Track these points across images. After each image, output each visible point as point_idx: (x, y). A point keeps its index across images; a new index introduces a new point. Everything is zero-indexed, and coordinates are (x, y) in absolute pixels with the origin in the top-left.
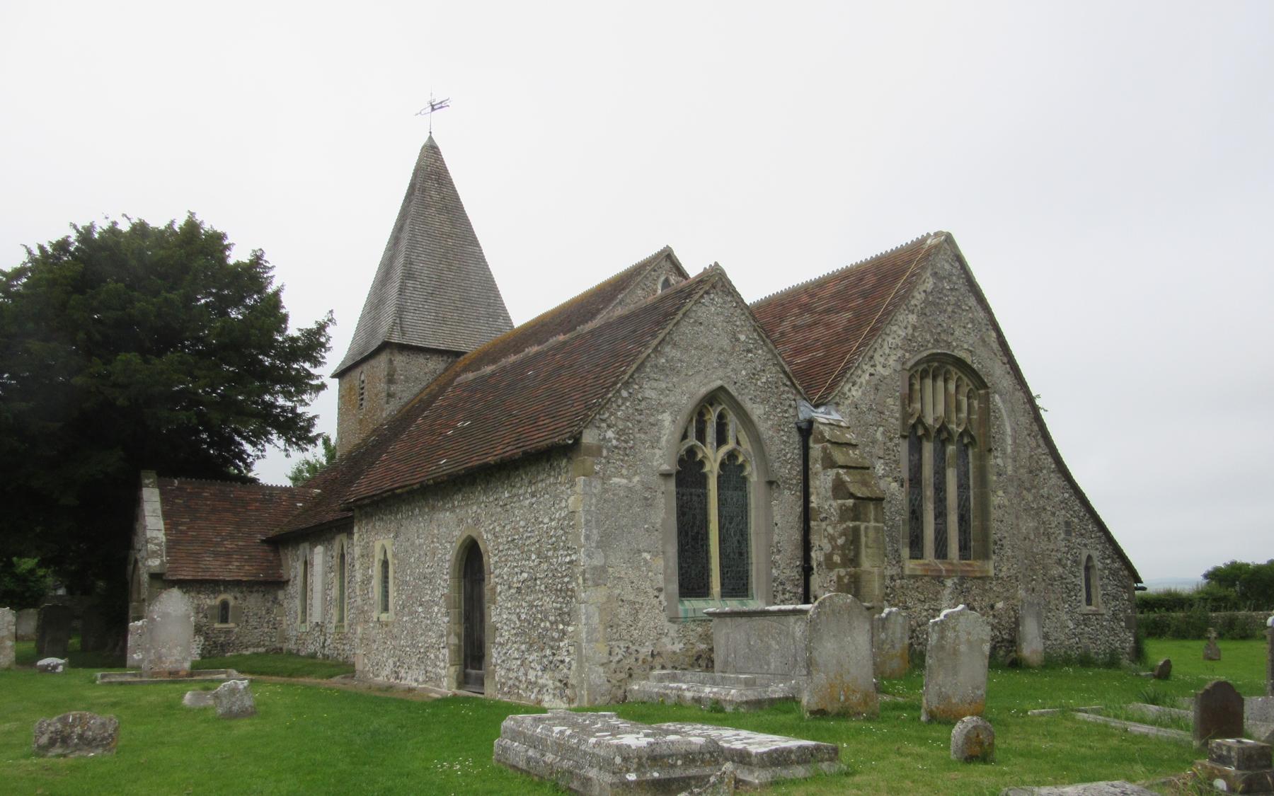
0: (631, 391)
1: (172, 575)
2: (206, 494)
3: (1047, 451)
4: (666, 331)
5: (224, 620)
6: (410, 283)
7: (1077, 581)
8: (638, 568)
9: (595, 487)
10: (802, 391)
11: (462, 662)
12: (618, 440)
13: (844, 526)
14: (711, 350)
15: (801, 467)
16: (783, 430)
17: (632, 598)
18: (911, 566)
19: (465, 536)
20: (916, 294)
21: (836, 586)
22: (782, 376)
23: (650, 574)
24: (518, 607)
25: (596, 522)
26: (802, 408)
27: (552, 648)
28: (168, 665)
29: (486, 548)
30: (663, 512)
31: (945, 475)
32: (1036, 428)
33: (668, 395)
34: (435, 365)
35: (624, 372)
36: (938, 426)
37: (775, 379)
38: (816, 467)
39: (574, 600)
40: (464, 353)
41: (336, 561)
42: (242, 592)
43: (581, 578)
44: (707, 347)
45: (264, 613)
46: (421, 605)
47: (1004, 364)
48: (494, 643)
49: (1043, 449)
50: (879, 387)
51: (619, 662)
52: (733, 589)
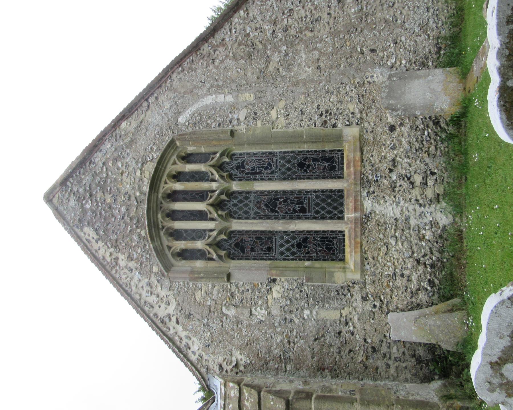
3: (227, 26)
47: (149, 106)
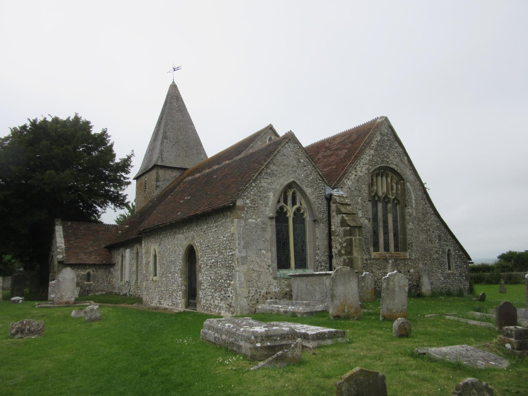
0: (256, 183)
1: (67, 262)
2: (81, 228)
3: (430, 206)
4: (271, 158)
5: (89, 280)
6: (165, 141)
7: (444, 260)
8: (260, 257)
9: (242, 223)
10: (327, 182)
11: (187, 297)
12: (251, 204)
13: (346, 238)
14: (289, 166)
15: (327, 214)
16: (319, 199)
17: (258, 269)
18: (374, 254)
19: (188, 244)
20: (373, 142)
21: (343, 263)
22: (318, 176)
23: (265, 259)
24: (210, 273)
25: (242, 238)
26: (327, 190)
27: (225, 291)
28: (65, 299)
29: (197, 249)
30: (270, 233)
31: (387, 216)
32: (425, 196)
33: (271, 185)
34: (176, 174)
35: (253, 176)
36: (384, 196)
37: (316, 178)
38: (334, 214)
39: (234, 270)
40: (187, 169)
41: (135, 255)
42: (96, 269)
43: (236, 261)
44: (287, 165)
45: (105, 277)
46: (170, 273)
47: (411, 170)
48: (200, 289)
49: (428, 205)
50: (359, 181)
51: (253, 296)
52: (300, 265)
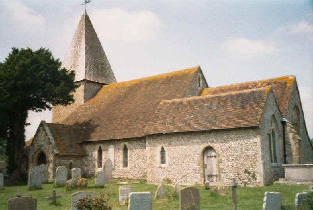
30: (268, 143)
